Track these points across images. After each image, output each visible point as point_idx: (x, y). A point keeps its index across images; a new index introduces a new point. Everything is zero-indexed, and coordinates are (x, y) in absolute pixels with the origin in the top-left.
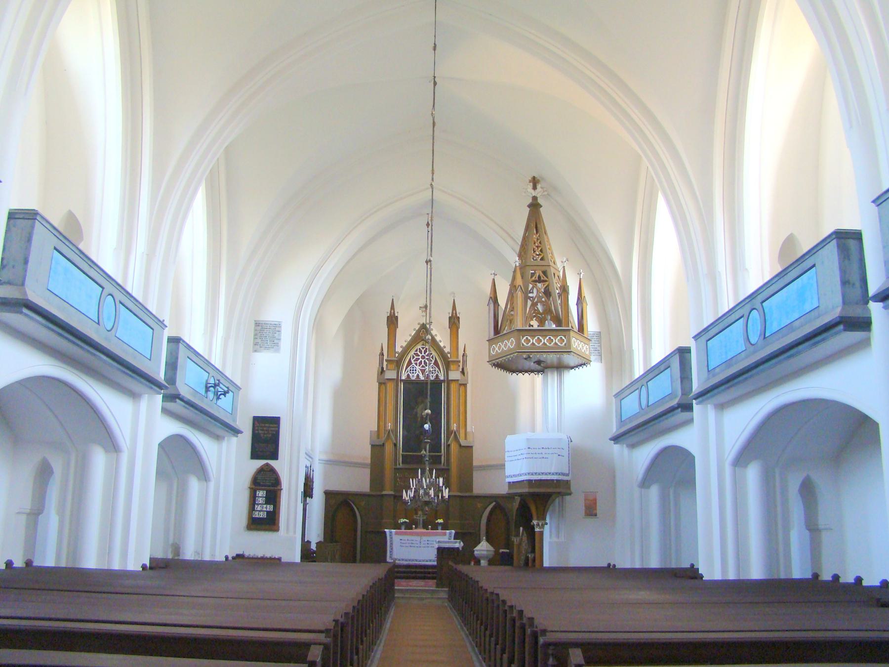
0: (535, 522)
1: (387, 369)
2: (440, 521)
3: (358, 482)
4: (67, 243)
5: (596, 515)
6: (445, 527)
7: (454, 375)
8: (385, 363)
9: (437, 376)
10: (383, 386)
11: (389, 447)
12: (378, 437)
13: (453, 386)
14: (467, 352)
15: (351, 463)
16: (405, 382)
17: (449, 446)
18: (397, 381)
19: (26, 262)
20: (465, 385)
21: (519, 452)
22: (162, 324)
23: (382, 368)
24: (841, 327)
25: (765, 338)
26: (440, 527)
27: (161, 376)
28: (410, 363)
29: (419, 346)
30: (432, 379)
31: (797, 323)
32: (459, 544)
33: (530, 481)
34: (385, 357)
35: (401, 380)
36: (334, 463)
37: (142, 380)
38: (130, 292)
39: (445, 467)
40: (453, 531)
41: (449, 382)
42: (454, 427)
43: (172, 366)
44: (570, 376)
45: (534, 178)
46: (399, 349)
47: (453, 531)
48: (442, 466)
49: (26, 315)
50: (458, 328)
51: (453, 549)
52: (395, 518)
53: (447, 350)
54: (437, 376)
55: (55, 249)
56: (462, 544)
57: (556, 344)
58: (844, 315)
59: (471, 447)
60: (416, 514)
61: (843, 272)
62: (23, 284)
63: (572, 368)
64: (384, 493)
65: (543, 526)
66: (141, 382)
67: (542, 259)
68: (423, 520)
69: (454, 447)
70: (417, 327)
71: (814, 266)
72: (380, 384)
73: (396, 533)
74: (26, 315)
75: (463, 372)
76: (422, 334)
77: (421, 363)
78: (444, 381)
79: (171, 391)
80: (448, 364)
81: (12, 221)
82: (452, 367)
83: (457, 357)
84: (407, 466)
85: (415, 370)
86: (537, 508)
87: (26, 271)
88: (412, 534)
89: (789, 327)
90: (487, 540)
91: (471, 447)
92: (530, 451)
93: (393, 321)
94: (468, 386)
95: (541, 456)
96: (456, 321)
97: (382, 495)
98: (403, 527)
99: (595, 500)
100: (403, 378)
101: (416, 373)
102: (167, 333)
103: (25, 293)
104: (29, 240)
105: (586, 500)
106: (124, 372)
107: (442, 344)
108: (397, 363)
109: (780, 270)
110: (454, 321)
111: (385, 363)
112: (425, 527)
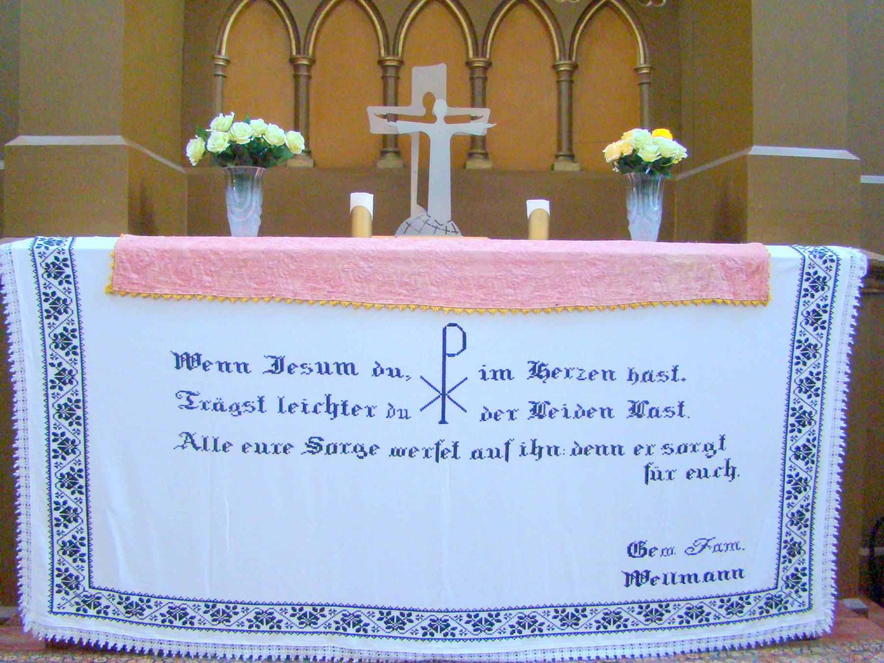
6: (710, 209)
26: (646, 212)
40: (852, 261)
60: (391, 86)
68: (467, 149)
73: (127, 281)
88: (328, 290)
112: (484, 208)
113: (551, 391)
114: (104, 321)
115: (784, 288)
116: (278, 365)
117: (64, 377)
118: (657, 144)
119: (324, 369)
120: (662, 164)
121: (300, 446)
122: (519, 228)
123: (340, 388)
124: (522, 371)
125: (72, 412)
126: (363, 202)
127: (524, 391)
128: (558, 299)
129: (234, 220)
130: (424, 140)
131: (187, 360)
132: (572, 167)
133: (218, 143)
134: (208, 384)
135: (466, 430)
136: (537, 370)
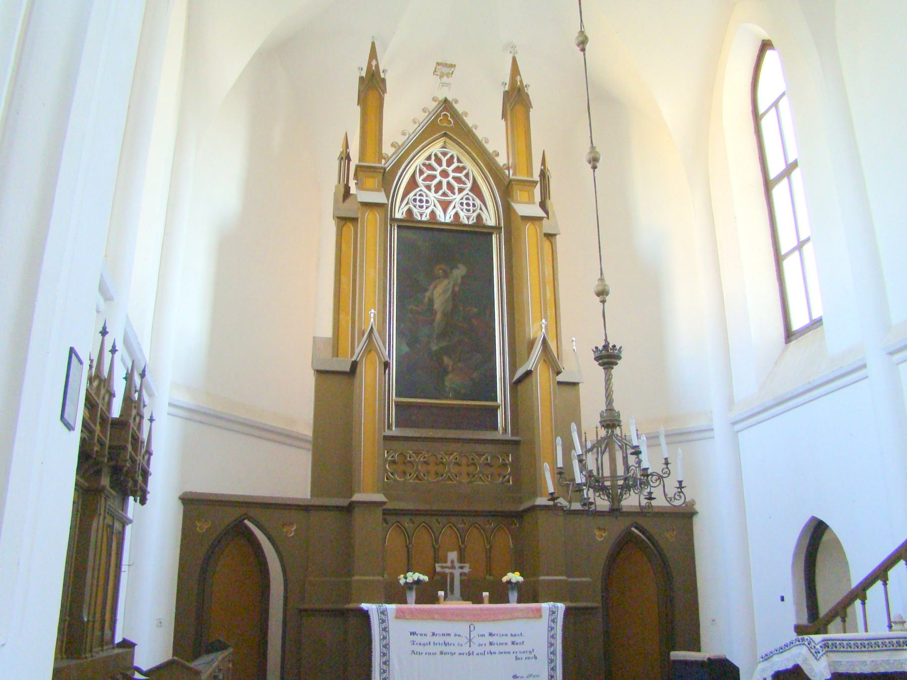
2: (515, 577)
9: (479, 217)
10: (350, 226)
11: (369, 374)
12: (336, 353)
14: (549, 165)
23: (347, 189)
26: (513, 595)
29: (436, 148)
34: (355, 161)
35: (393, 220)
36: (209, 418)
39: (509, 436)
40: (561, 606)
47: (561, 606)
48: (499, 435)
53: (502, 160)
54: (479, 217)
69: (542, 382)
70: (433, 105)
72: (343, 220)
73: (400, 615)
76: (447, 123)
77: (439, 186)
78: (497, 228)
82: (519, 193)
85: (421, 202)
88: (430, 616)
91: (575, 384)
93: (372, 86)
97: (350, 508)
98: (412, 596)
100: (399, 215)
101: (430, 206)
107: (490, 148)
108: (387, 179)
110: (516, 99)
112: (471, 593)
113: (494, 639)
114: (394, 625)
115: (546, 614)
116: (433, 634)
117: (384, 638)
118: (515, 577)
119: (443, 635)
120: (517, 583)
121: (438, 653)
123: (448, 639)
124: (487, 635)
125: (386, 646)
126: (441, 593)
127: (489, 639)
128: (494, 617)
129: (409, 599)
130: (452, 575)
131: (413, 634)
132: (491, 578)
133: (410, 580)
134: (417, 639)
135: (476, 649)
136: (490, 634)
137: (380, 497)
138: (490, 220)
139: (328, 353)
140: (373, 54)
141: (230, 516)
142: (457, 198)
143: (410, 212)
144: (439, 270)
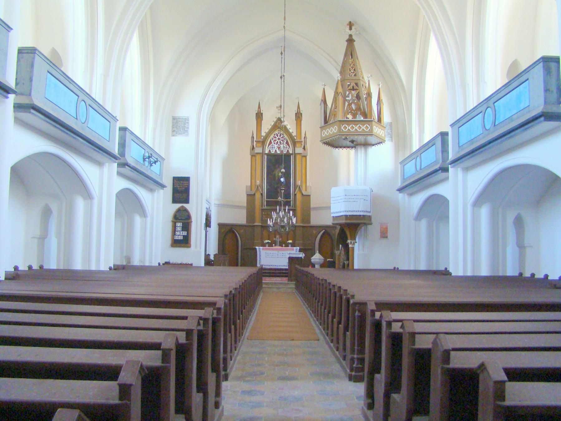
0: (349, 241)
1: (256, 146)
2: (290, 241)
3: (239, 218)
4: (55, 68)
5: (387, 237)
6: (293, 245)
7: (299, 150)
8: (255, 143)
9: (288, 151)
10: (254, 157)
11: (258, 196)
12: (251, 190)
13: (298, 157)
15: (235, 206)
16: (268, 155)
17: (295, 195)
18: (263, 154)
19: (31, 80)
20: (305, 157)
21: (340, 198)
22: (115, 119)
23: (253, 146)
24: (542, 119)
25: (495, 125)
26: (290, 245)
27: (116, 152)
28: (271, 142)
29: (277, 132)
30: (285, 153)
31: (515, 116)
32: (302, 255)
33: (346, 216)
34: (255, 139)
36: (223, 206)
37: (104, 154)
38: (94, 98)
41: (295, 155)
42: (299, 183)
43: (123, 145)
44: (372, 150)
45: (350, 22)
46: (263, 134)
49: (33, 114)
50: (301, 121)
51: (298, 258)
52: (262, 239)
53: (294, 134)
54: (288, 151)
55: (48, 72)
56: (304, 255)
57: (363, 129)
58: (545, 111)
59: (309, 196)
60: (275, 237)
61: (546, 83)
62: (30, 95)
63: (373, 145)
64: (255, 224)
65: (354, 244)
66: (104, 155)
67: (355, 75)
69: (299, 196)
70: (275, 120)
71: (528, 79)
72: (253, 156)
73: (263, 249)
74: (33, 114)
75: (304, 148)
76: (278, 125)
77: (277, 142)
78: (292, 154)
79: (122, 161)
80: (294, 143)
81: (20, 55)
82: (298, 145)
83: (301, 139)
84: (269, 208)
86: (350, 234)
87: (31, 86)
88: (272, 250)
89: (510, 119)
90: (320, 253)
91: (309, 196)
92: (346, 197)
93: (259, 116)
94: (308, 157)
95: (353, 200)
96: (300, 116)
98: (267, 245)
99: (387, 228)
100: (267, 152)
101: (274, 149)
102: (119, 125)
103: (32, 100)
104: (32, 66)
105: (381, 228)
106: (94, 150)
107: (291, 131)
108: (263, 143)
109: (507, 81)
110: (299, 116)
111: (255, 143)
114: (262, 251)
122: (282, 246)
128: (284, 250)
137: (260, 224)
138: (291, 152)
139: (249, 190)
140: (259, 107)
141: (229, 228)
142: (282, 146)
143: (270, 151)
144: (277, 166)
